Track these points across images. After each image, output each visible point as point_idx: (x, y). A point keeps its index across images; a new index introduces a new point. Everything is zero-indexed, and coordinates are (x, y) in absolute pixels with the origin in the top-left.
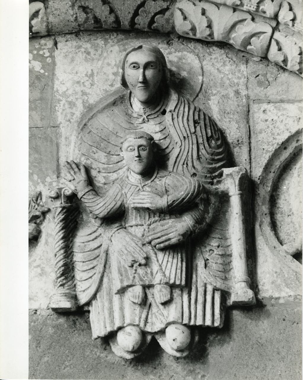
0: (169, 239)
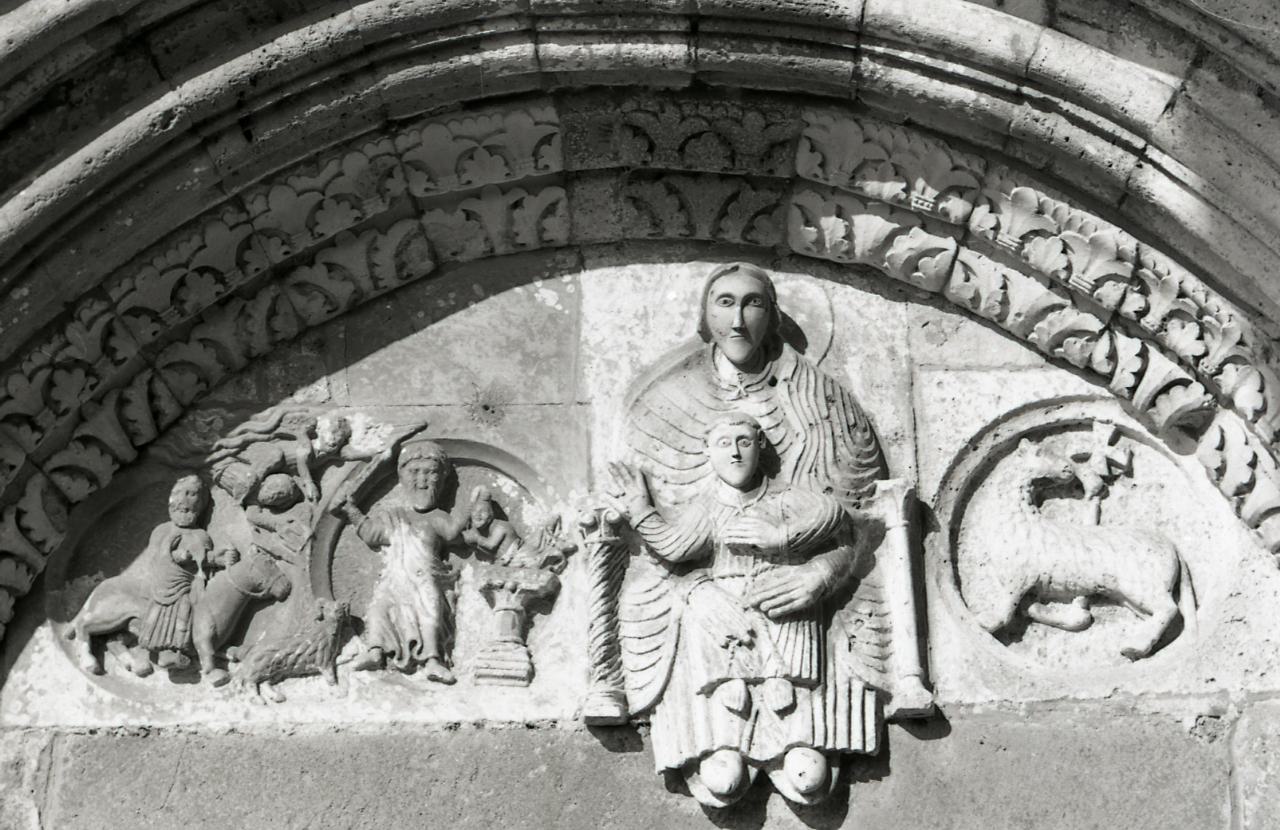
0: (792, 601)
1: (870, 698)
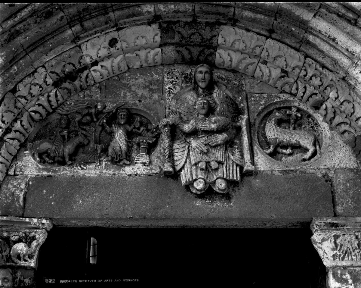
1: (238, 168)
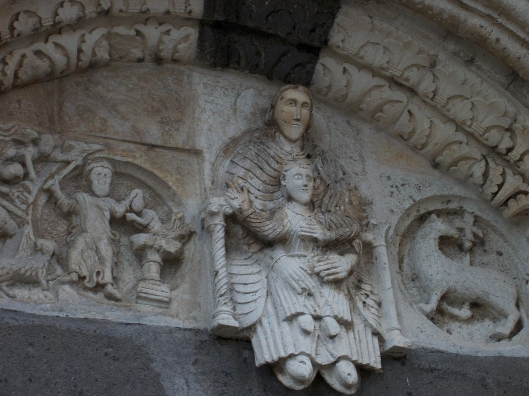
0: (337, 273)
